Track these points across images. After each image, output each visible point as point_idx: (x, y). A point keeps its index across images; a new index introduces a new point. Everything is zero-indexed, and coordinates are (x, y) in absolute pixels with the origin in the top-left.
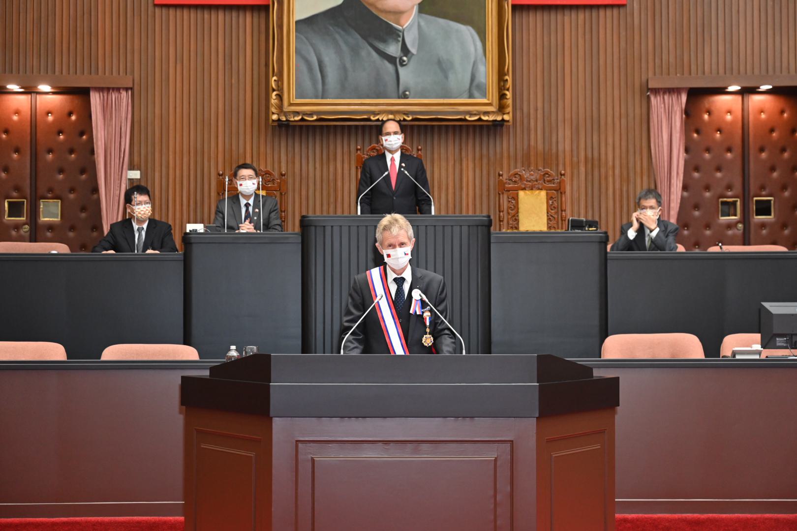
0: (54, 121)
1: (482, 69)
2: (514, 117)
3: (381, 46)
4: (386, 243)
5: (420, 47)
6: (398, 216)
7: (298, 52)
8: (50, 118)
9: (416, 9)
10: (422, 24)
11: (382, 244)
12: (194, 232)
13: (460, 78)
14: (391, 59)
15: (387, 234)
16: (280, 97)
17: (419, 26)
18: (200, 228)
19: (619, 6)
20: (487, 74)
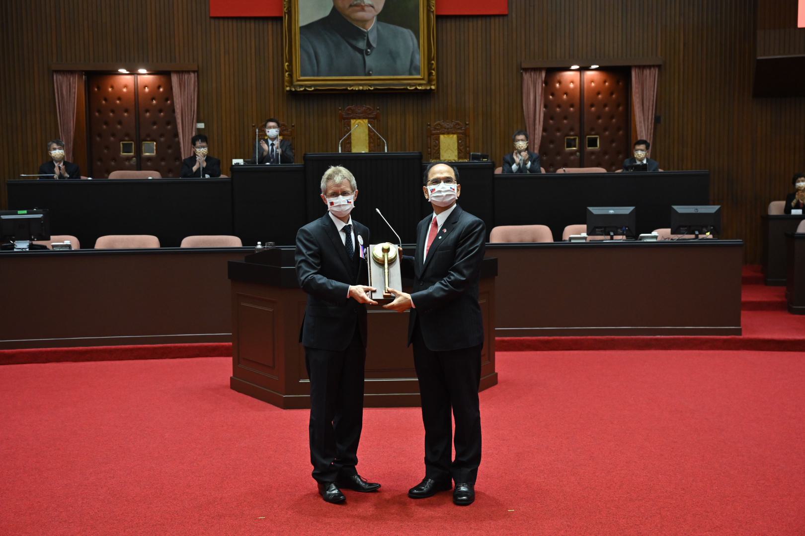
0: (150, 92)
1: (417, 57)
2: (438, 87)
3: (354, 43)
4: (330, 192)
5: (378, 44)
6: (342, 168)
7: (301, 46)
8: (147, 90)
9: (375, 19)
10: (380, 28)
11: (325, 194)
12: (237, 164)
13: (403, 62)
14: (360, 51)
15: (330, 183)
16: (291, 76)
17: (378, 30)
18: (241, 161)
19: (503, 16)
20: (420, 59)
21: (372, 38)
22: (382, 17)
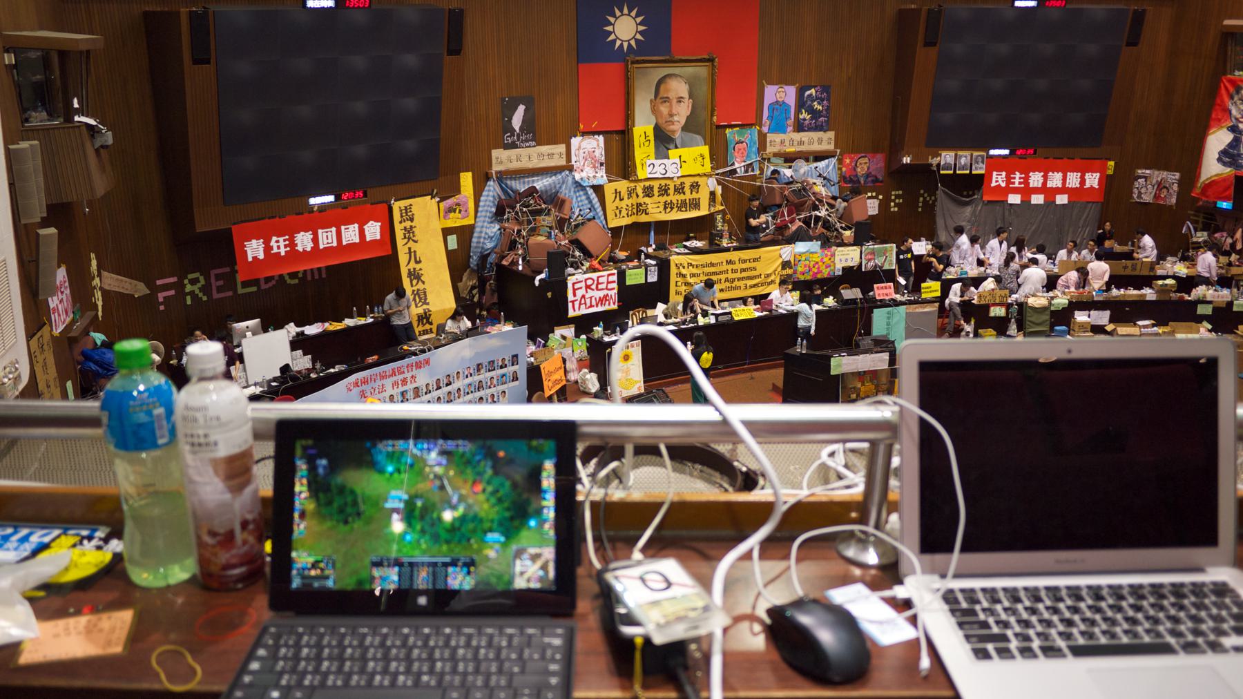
21: (678, 142)
22: (684, 129)
